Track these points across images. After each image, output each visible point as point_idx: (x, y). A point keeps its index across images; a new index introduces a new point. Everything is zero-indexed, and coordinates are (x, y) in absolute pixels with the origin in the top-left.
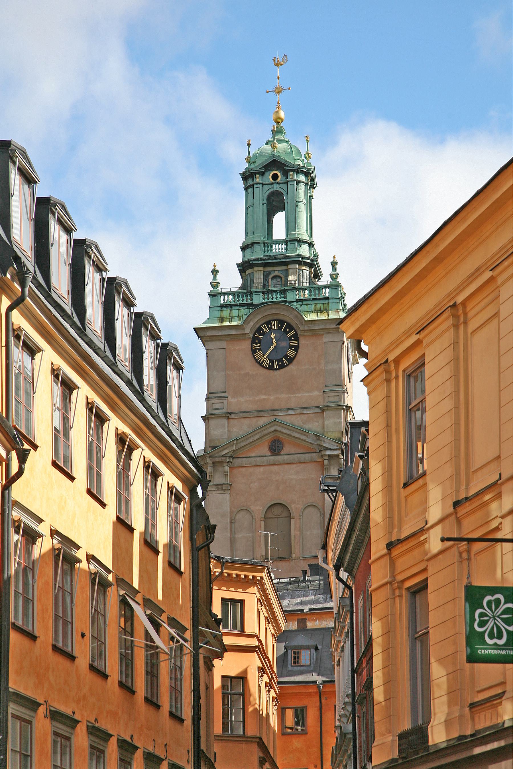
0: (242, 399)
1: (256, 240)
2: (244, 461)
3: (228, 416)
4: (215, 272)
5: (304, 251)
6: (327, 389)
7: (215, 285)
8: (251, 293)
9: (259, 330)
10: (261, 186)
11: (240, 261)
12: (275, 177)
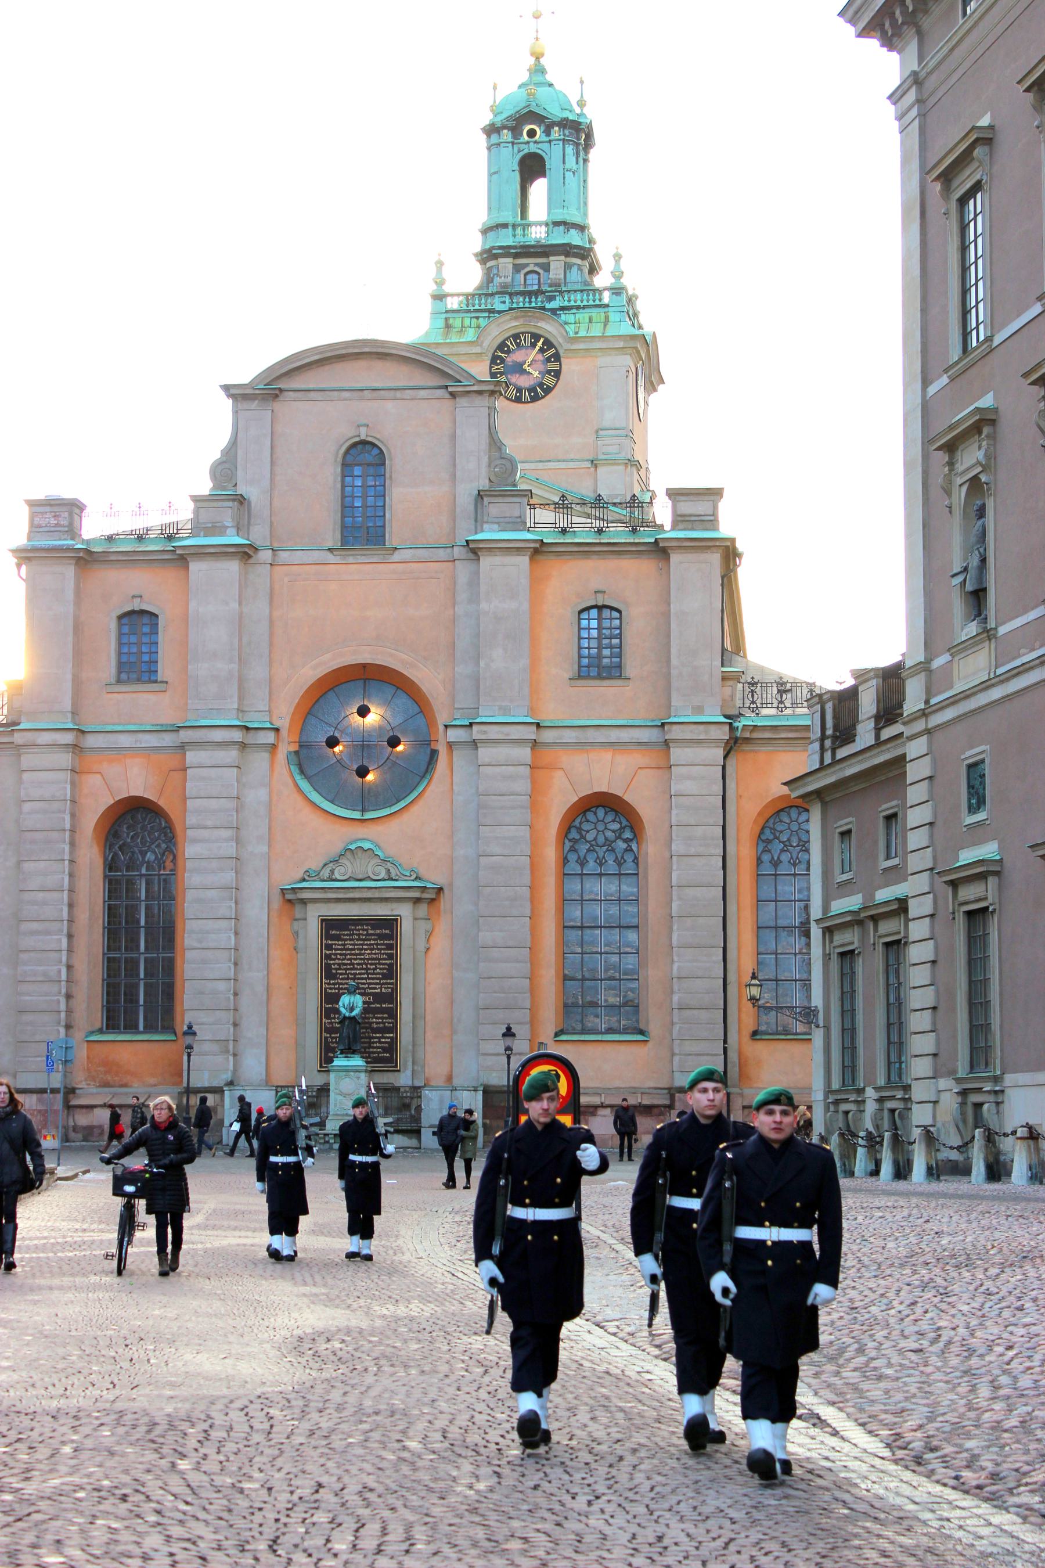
1: (501, 221)
4: (440, 264)
5: (574, 238)
7: (440, 282)
9: (502, 346)
10: (510, 145)
11: (478, 249)
12: (532, 133)
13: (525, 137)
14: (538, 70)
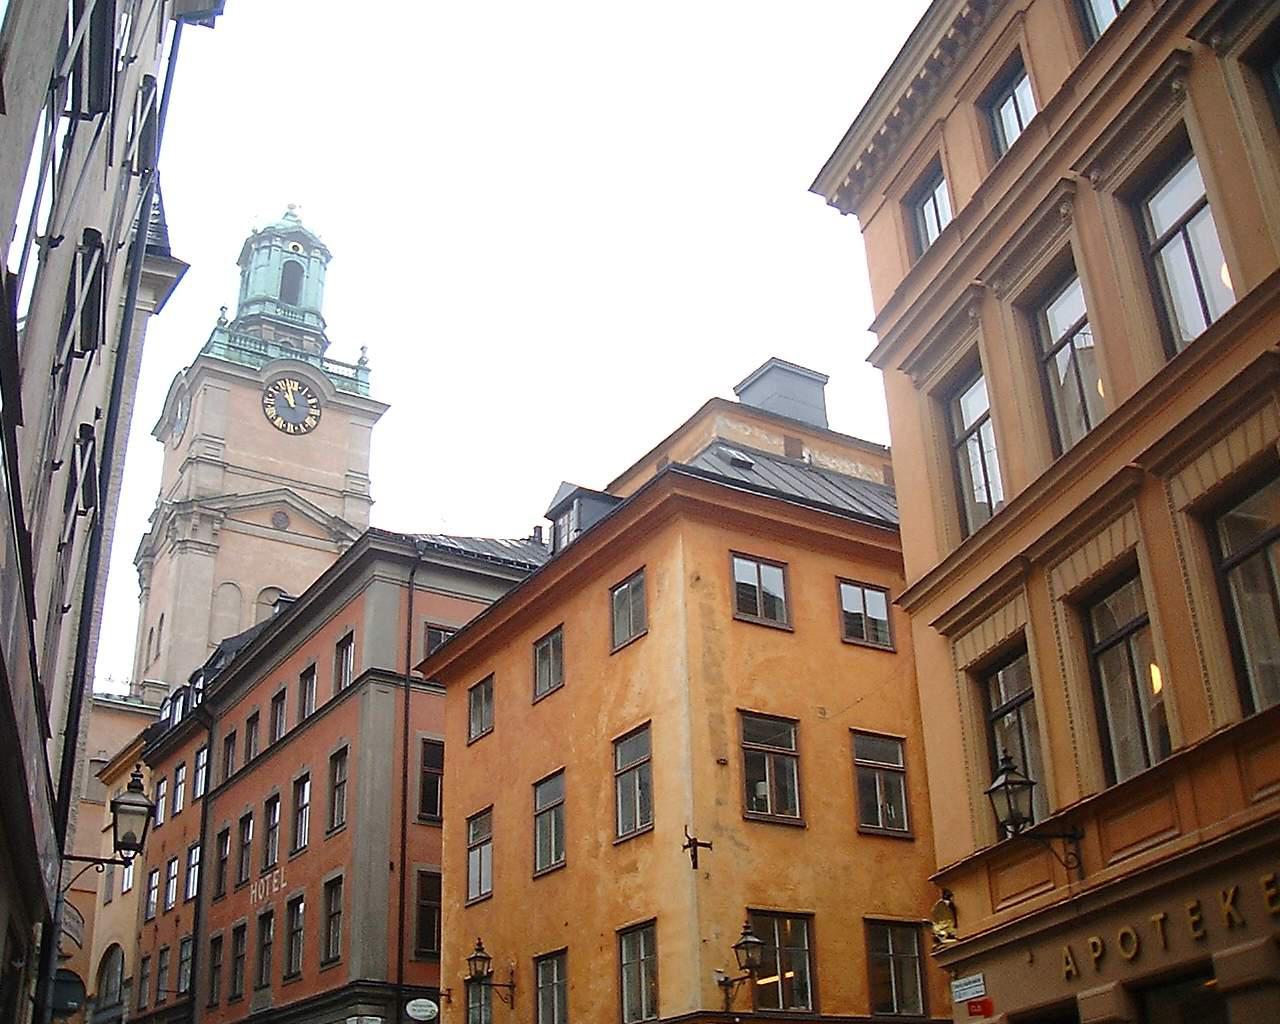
0: (244, 454)
2: (239, 526)
6: (349, 473)
8: (266, 345)
13: (291, 250)
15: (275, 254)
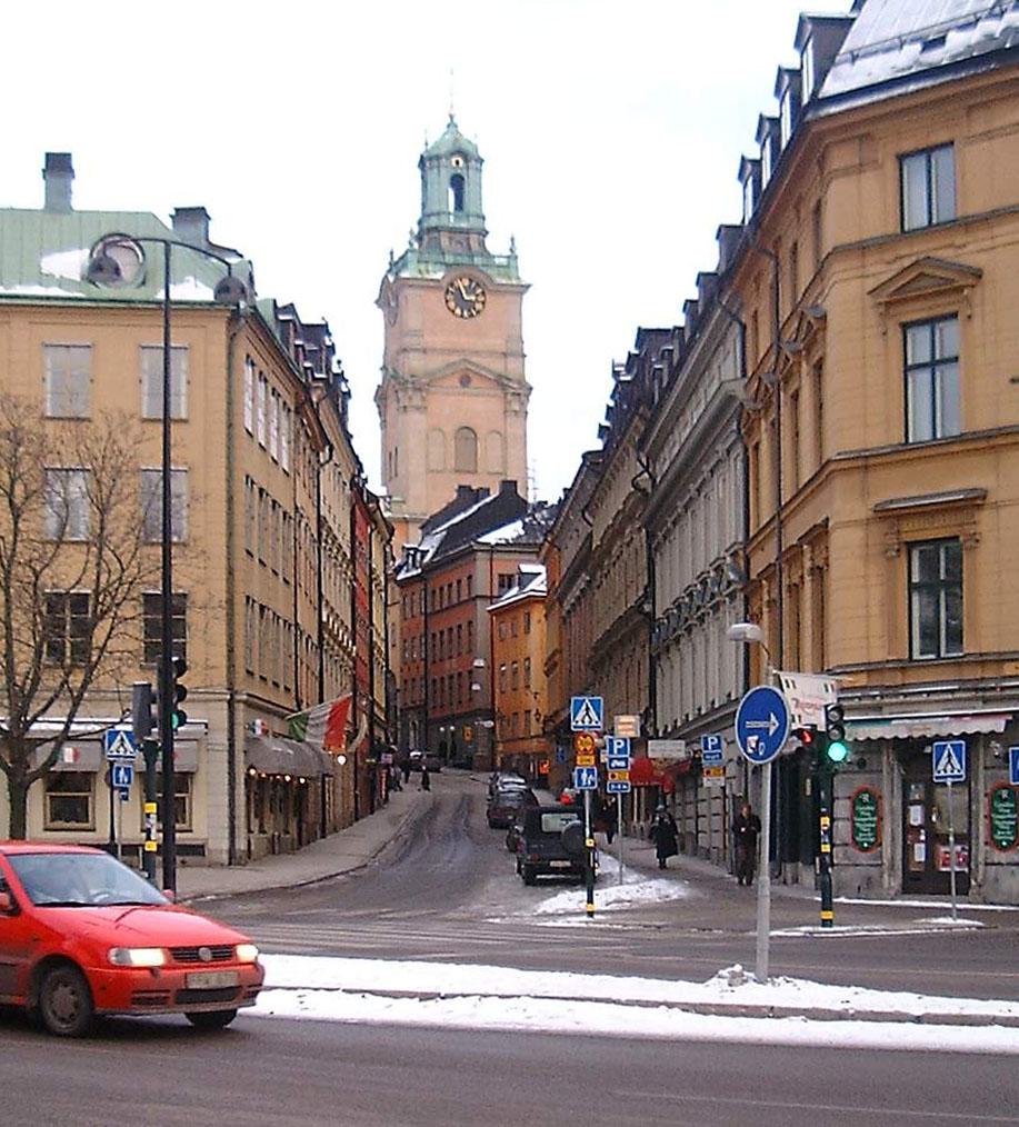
3: (425, 351)
12: (457, 162)
14: (452, 125)
15: (443, 171)
